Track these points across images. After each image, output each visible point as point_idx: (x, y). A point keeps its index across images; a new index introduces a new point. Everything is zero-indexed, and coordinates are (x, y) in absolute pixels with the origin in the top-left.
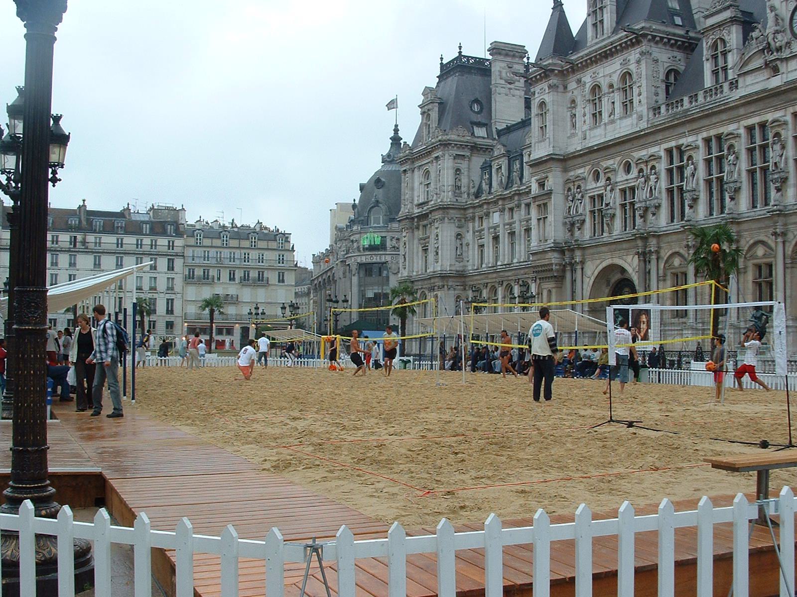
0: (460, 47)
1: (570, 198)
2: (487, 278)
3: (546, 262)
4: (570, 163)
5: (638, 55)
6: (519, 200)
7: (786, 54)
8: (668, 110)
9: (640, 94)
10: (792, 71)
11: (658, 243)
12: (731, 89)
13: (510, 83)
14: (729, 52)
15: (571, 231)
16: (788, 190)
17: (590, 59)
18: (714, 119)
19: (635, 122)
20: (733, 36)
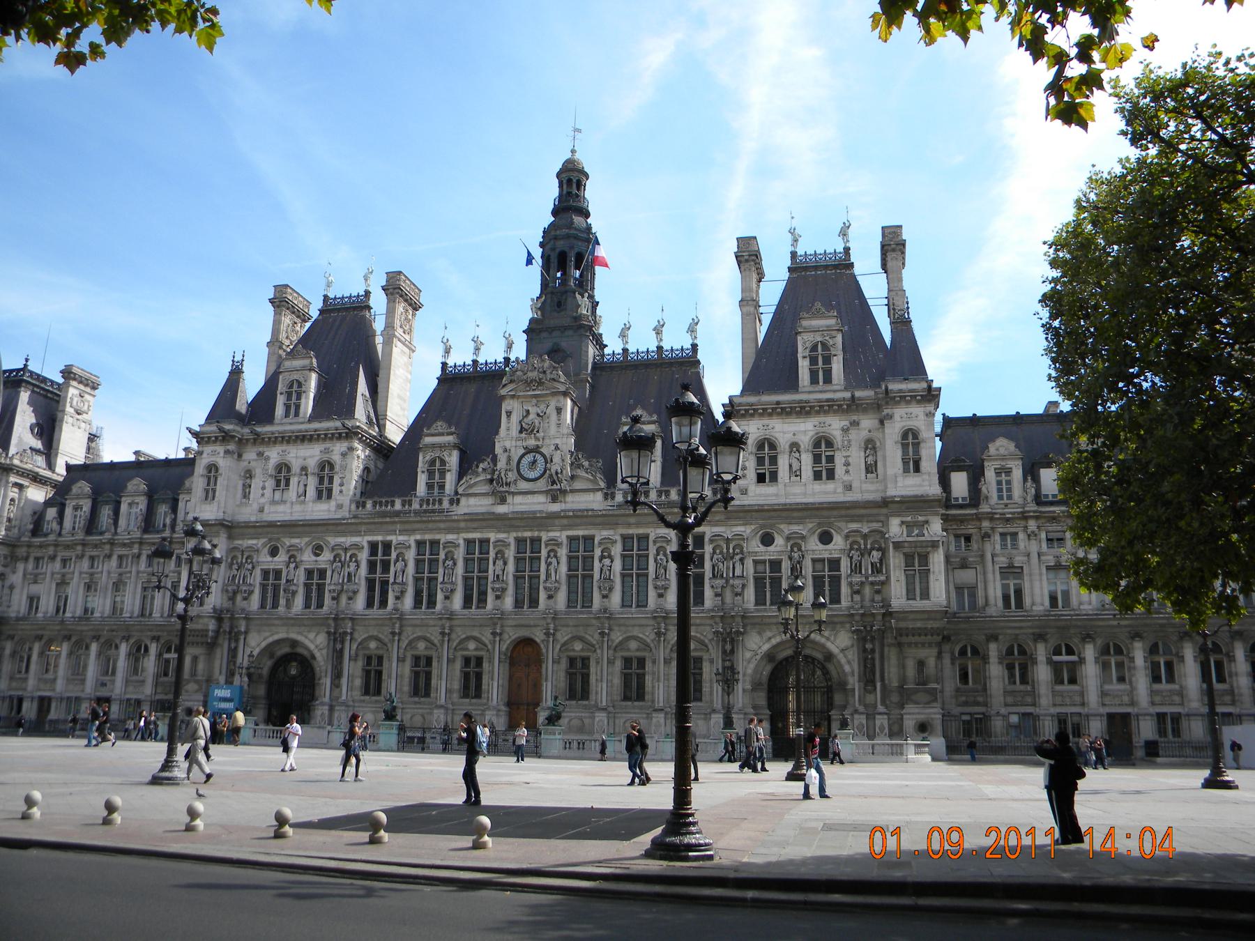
0: (27, 360)
1: (235, 566)
2: (44, 629)
3: (199, 627)
4: (237, 531)
5: (345, 449)
6: (112, 550)
8: (374, 506)
9: (342, 485)
11: (353, 624)
13: (79, 414)
15: (232, 599)
17: (283, 437)
18: (430, 525)
19: (333, 509)
20: (453, 459)
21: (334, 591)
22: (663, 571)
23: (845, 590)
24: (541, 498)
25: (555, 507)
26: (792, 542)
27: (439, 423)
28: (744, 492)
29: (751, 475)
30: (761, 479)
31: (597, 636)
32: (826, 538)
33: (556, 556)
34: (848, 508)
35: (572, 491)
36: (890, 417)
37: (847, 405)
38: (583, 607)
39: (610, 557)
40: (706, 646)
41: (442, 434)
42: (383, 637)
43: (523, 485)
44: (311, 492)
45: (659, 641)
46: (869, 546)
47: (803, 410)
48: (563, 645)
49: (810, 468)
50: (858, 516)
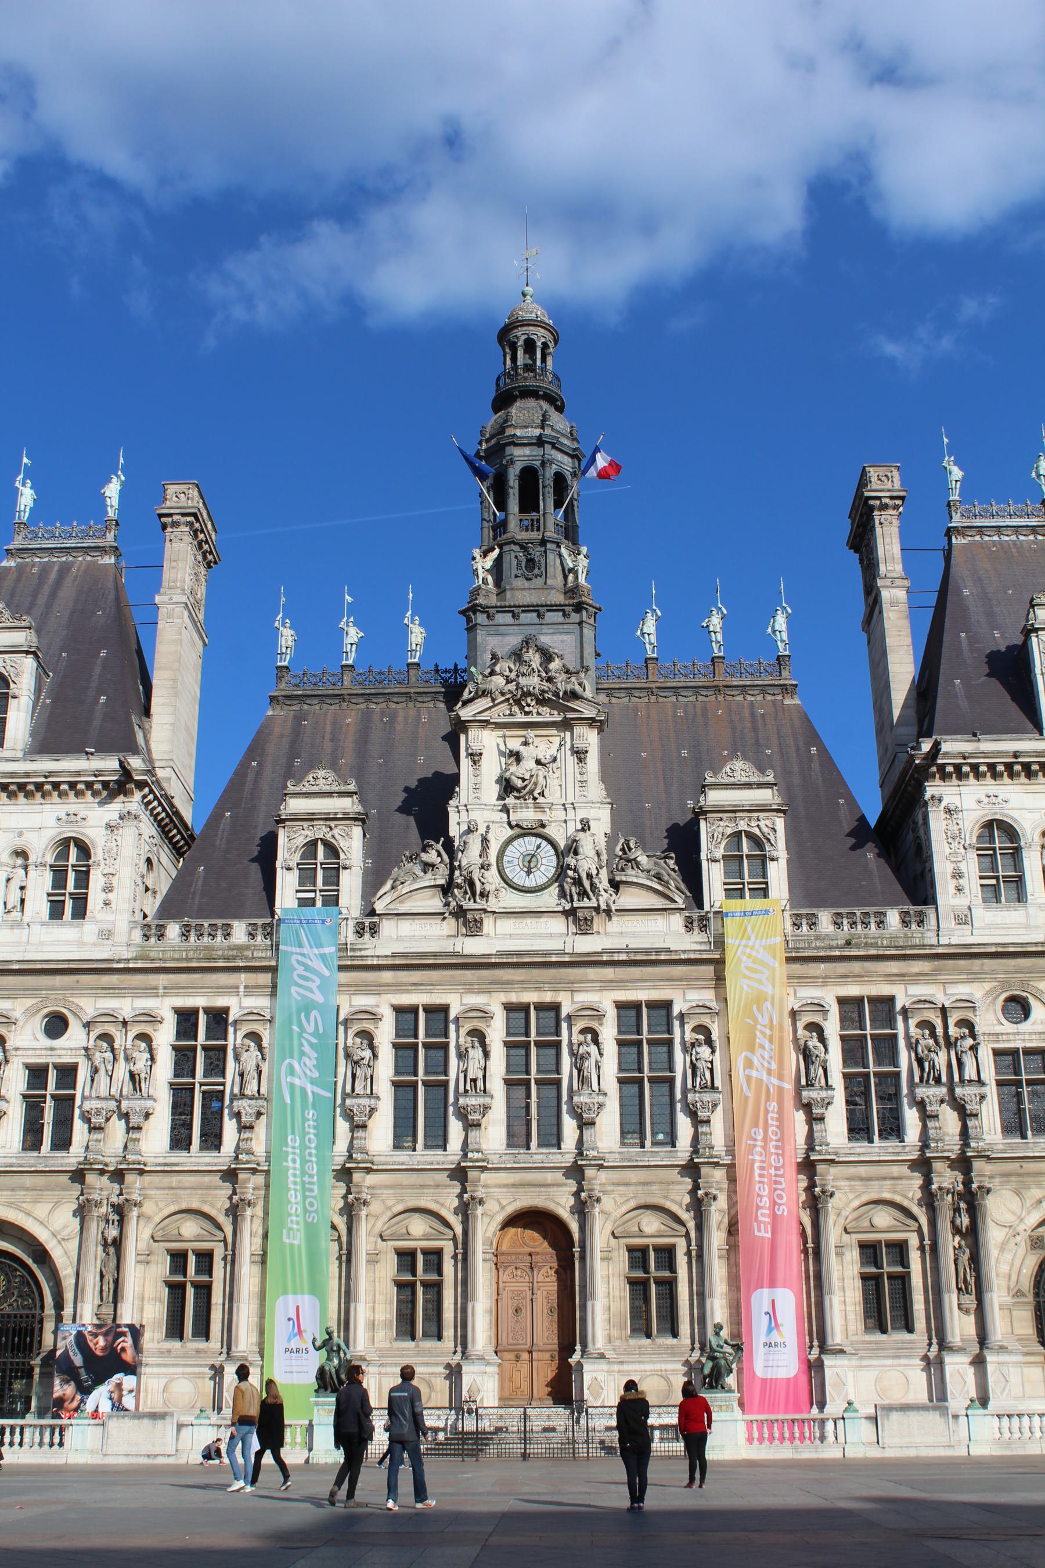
7: (493, 904)
8: (185, 935)
9: (108, 889)
12: (360, 933)
14: (345, 868)
16: (490, 1128)
21: (98, 1113)
22: (821, 1071)
25: (586, 945)
27: (321, 773)
28: (964, 920)
29: (973, 882)
30: (992, 894)
33: (596, 1041)
38: (654, 1144)
39: (709, 1042)
40: (916, 1219)
41: (329, 794)
42: (213, 1213)
43: (512, 900)
44: (38, 904)
45: (825, 1208)
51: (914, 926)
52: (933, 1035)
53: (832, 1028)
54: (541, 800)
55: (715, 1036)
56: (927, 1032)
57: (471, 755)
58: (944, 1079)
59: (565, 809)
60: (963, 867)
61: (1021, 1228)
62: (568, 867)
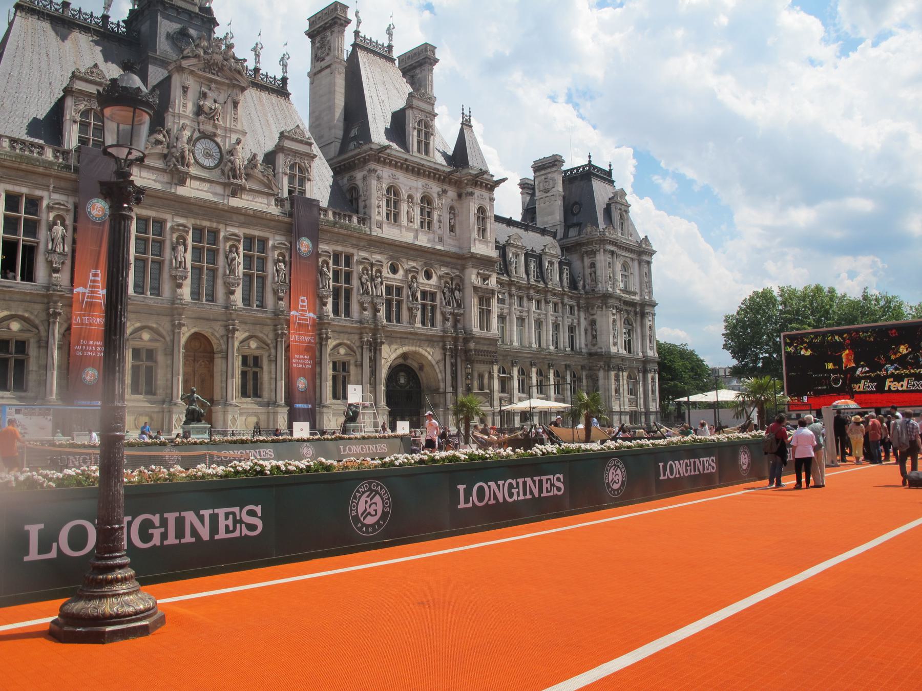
10: (194, 189)
23: (439, 317)
24: (219, 189)
25: (235, 202)
26: (411, 274)
28: (380, 226)
29: (384, 210)
31: (271, 335)
32: (428, 276)
34: (442, 255)
35: (251, 190)
36: (472, 194)
37: (444, 176)
40: (355, 352)
42: (32, 317)
46: (454, 287)
47: (417, 170)
48: (242, 342)
49: (419, 217)
50: (447, 263)
51: (362, 225)
52: (367, 274)
53: (331, 262)
54: (216, 122)
55: (287, 259)
56: (365, 272)
57: (183, 87)
58: (371, 293)
59: (226, 130)
60: (381, 202)
61: (389, 359)
62: (230, 161)
